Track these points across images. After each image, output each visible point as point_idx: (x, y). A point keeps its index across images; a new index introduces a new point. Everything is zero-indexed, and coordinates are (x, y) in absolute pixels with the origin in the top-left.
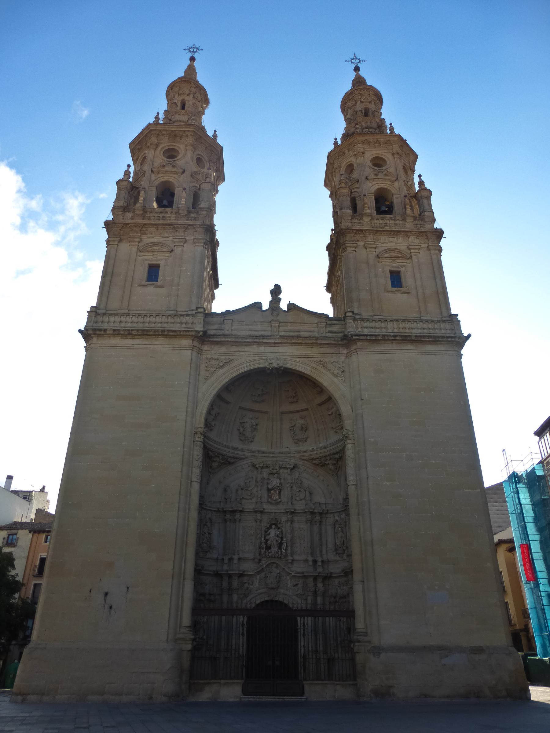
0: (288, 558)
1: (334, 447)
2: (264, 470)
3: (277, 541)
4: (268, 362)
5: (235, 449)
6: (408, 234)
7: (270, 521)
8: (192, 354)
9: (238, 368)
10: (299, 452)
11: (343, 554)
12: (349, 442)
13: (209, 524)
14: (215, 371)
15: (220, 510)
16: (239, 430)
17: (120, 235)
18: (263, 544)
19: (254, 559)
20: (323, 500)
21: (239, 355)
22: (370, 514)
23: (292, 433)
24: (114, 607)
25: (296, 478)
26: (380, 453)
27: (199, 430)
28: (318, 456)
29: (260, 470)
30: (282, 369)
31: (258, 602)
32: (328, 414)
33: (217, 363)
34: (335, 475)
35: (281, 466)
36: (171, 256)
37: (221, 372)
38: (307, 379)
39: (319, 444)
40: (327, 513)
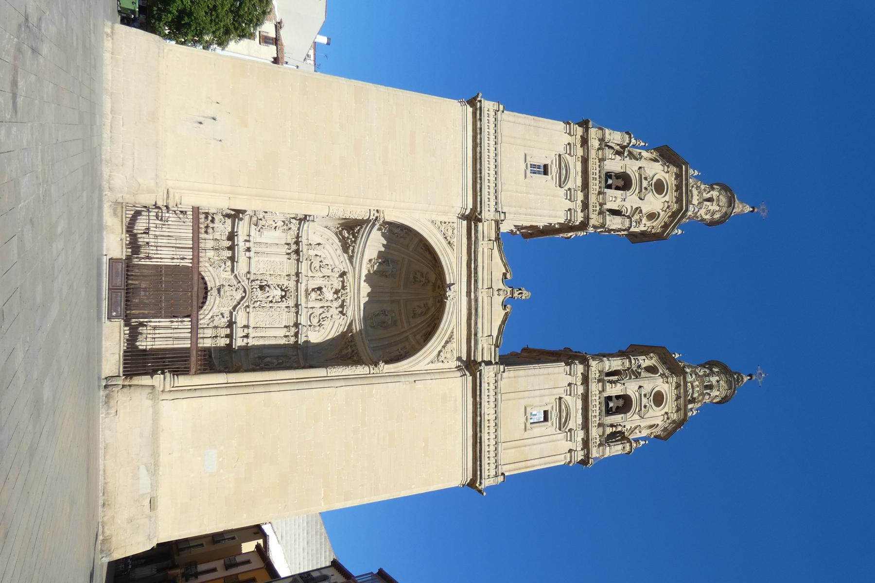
2: (341, 283)
4: (452, 285)
7: (289, 290)
9: (445, 255)
12: (371, 369)
17: (576, 135)
21: (458, 256)
24: (201, 126)
26: (360, 400)
27: (382, 215)
29: (341, 279)
30: (445, 300)
31: (206, 278)
36: (556, 187)
37: (441, 238)
38: (434, 327)
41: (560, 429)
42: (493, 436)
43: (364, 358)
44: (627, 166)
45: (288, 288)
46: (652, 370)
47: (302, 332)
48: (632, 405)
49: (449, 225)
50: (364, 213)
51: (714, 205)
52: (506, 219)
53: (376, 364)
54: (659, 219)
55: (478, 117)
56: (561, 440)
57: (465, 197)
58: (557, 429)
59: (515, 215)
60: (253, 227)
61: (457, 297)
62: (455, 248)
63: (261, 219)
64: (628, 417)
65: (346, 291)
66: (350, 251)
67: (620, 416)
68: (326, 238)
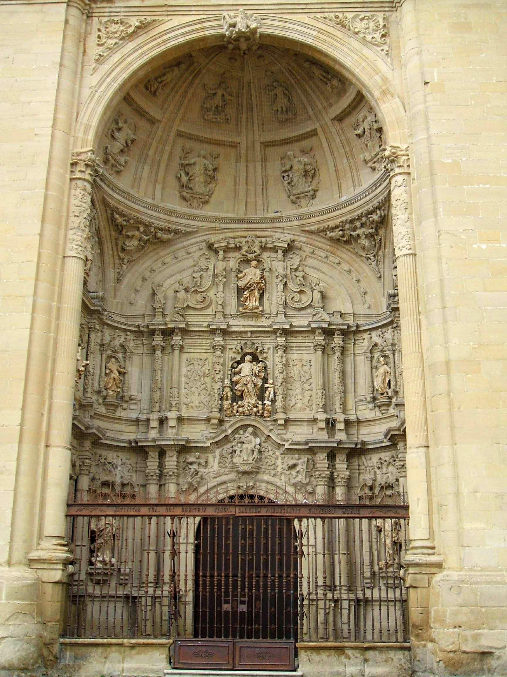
0: (276, 416)
1: (368, 198)
2: (231, 255)
3: (255, 384)
5: (170, 212)
7: (241, 348)
9: (165, 38)
10: (301, 217)
11: (389, 405)
12: (397, 170)
13: (120, 355)
14: (116, 43)
16: (179, 179)
18: (228, 389)
19: (208, 420)
20: (347, 308)
23: (287, 182)
25: (295, 267)
27: (82, 157)
28: (337, 222)
29: (221, 253)
32: (356, 135)
33: (122, 28)
34: (372, 258)
35: (263, 246)
37: (131, 46)
47: (325, 322)
50: (79, 191)
60: (120, 413)
62: (149, 19)
63: (105, 398)
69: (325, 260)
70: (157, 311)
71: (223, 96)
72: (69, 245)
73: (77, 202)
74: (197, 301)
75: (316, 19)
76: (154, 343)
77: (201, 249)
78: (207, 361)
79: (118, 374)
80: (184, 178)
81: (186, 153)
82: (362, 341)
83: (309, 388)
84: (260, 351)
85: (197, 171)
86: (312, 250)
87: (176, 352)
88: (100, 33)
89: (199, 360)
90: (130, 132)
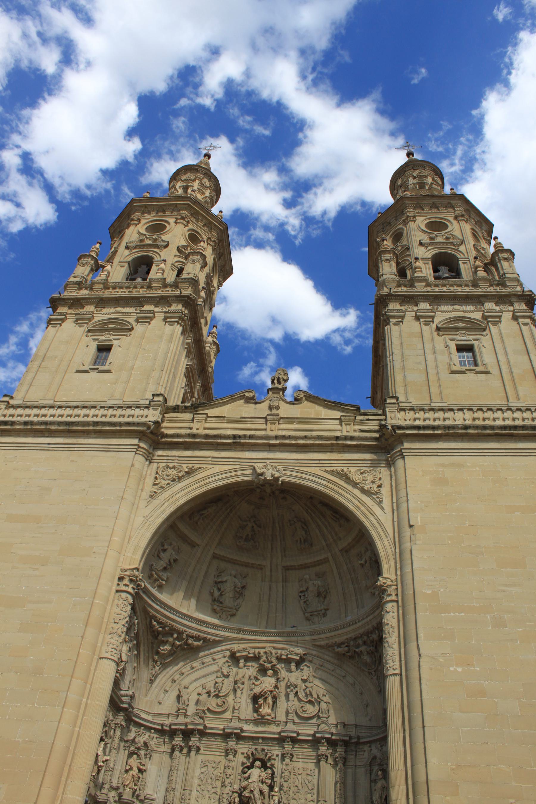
4: (256, 472)
6: (482, 300)
7: (252, 754)
8: (134, 457)
9: (207, 481)
13: (142, 752)
14: (168, 484)
15: (165, 728)
16: (212, 594)
18: (236, 795)
21: (210, 462)
22: (424, 727)
26: (443, 615)
29: (242, 661)
30: (280, 482)
37: (179, 486)
38: (326, 505)
39: (346, 617)
40: (358, 743)
41: (484, 330)
42: (499, 414)
43: (374, 623)
44: (122, 260)
45: (248, 755)
46: (398, 237)
48: (445, 253)
49: (160, 473)
50: (121, 601)
51: (192, 184)
52: (162, 393)
53: (383, 591)
54: (198, 231)
55: (8, 427)
56: (499, 329)
57: (119, 448)
58: (484, 333)
59: (161, 384)
61: (276, 465)
62: (196, 466)
64: (462, 256)
65: (262, 654)
66: (196, 643)
67: (462, 266)
68: (170, 684)
69: (333, 673)
70: (181, 711)
71: (253, 527)
72: (104, 648)
73: (118, 611)
74: (218, 705)
75: (326, 471)
76: (174, 743)
77: (224, 657)
78: (220, 764)
79: (137, 771)
80: (216, 594)
81: (220, 573)
82: (362, 753)
83: (311, 798)
84: (270, 757)
85: (228, 588)
86: (321, 663)
87: (193, 753)
88: (157, 476)
89: (213, 762)
90: (174, 553)
